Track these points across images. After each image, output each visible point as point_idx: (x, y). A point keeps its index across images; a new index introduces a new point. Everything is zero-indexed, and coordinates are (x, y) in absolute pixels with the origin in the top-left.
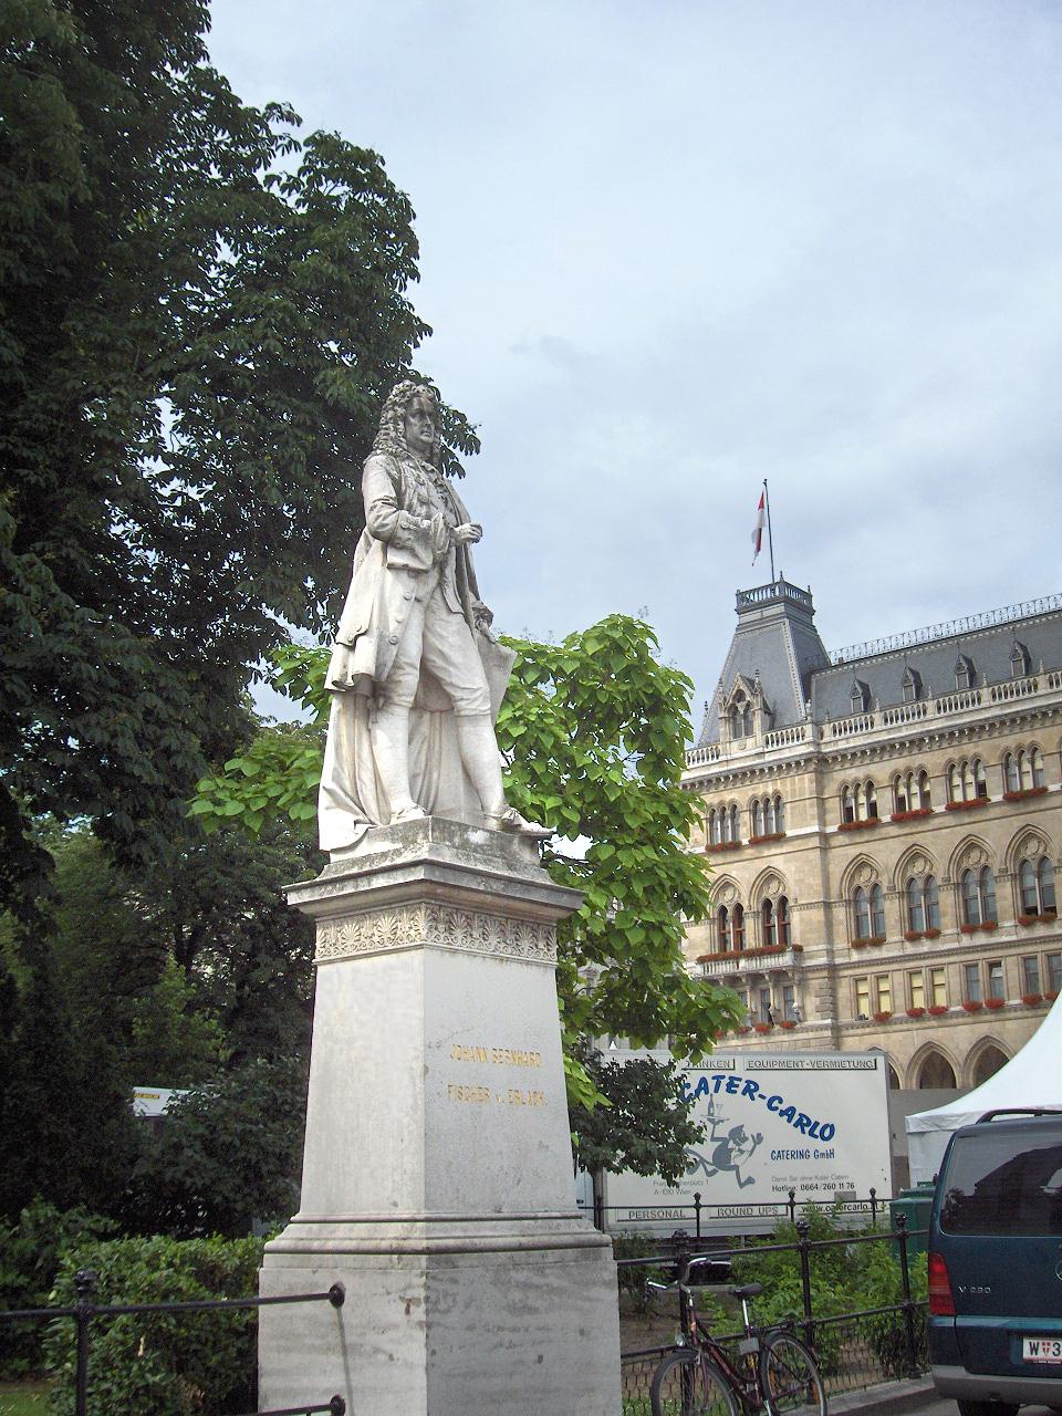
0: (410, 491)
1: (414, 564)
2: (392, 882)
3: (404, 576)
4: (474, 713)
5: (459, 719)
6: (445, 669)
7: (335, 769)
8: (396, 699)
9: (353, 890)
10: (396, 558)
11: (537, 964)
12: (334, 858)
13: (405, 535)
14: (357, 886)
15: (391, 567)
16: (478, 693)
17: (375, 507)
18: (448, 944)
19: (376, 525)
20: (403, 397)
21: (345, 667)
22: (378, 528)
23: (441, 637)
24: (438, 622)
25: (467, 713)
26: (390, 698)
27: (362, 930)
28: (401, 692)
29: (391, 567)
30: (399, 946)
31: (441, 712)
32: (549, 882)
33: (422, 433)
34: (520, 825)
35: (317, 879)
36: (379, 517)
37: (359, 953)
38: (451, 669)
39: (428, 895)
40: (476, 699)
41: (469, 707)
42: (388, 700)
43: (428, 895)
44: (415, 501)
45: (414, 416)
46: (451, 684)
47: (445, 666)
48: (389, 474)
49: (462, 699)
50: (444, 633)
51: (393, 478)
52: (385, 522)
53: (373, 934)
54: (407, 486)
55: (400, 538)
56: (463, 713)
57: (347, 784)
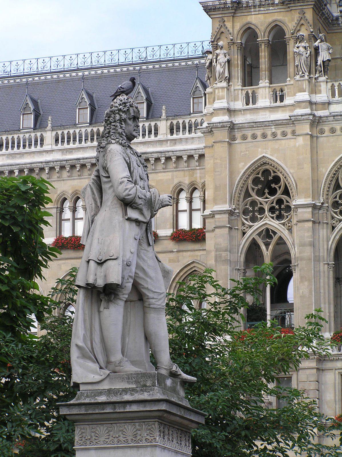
0: (135, 171)
1: (141, 218)
2: (145, 409)
3: (134, 224)
4: (158, 307)
5: (325, 373)
6: (144, 279)
7: (84, 334)
8: (121, 296)
9: (112, 411)
10: (133, 214)
11: (169, 450)
12: (82, 388)
13: (140, 202)
14: (115, 409)
15: (129, 219)
16: (162, 295)
17: (123, 182)
18: (164, 444)
19: (124, 194)
20: (125, 106)
21: (96, 275)
22: (125, 196)
23: (144, 260)
24: (142, 251)
25: (155, 306)
26: (118, 295)
27: (111, 433)
28: (124, 292)
29: (129, 219)
30: (139, 444)
31: (131, 301)
32: (189, 406)
33: (134, 130)
34: (180, 375)
35: (72, 402)
36: (127, 189)
37: (108, 446)
38: (149, 280)
39: (159, 418)
40: (161, 299)
41: (157, 303)
42: (116, 296)
43: (159, 418)
44: (138, 178)
45: (130, 119)
46: (147, 289)
47: (145, 277)
48: (125, 159)
49: (153, 298)
50: (145, 258)
51: (127, 163)
52: (130, 193)
53: (119, 436)
54: (134, 168)
55: (136, 203)
56: (151, 306)
57: (90, 346)
